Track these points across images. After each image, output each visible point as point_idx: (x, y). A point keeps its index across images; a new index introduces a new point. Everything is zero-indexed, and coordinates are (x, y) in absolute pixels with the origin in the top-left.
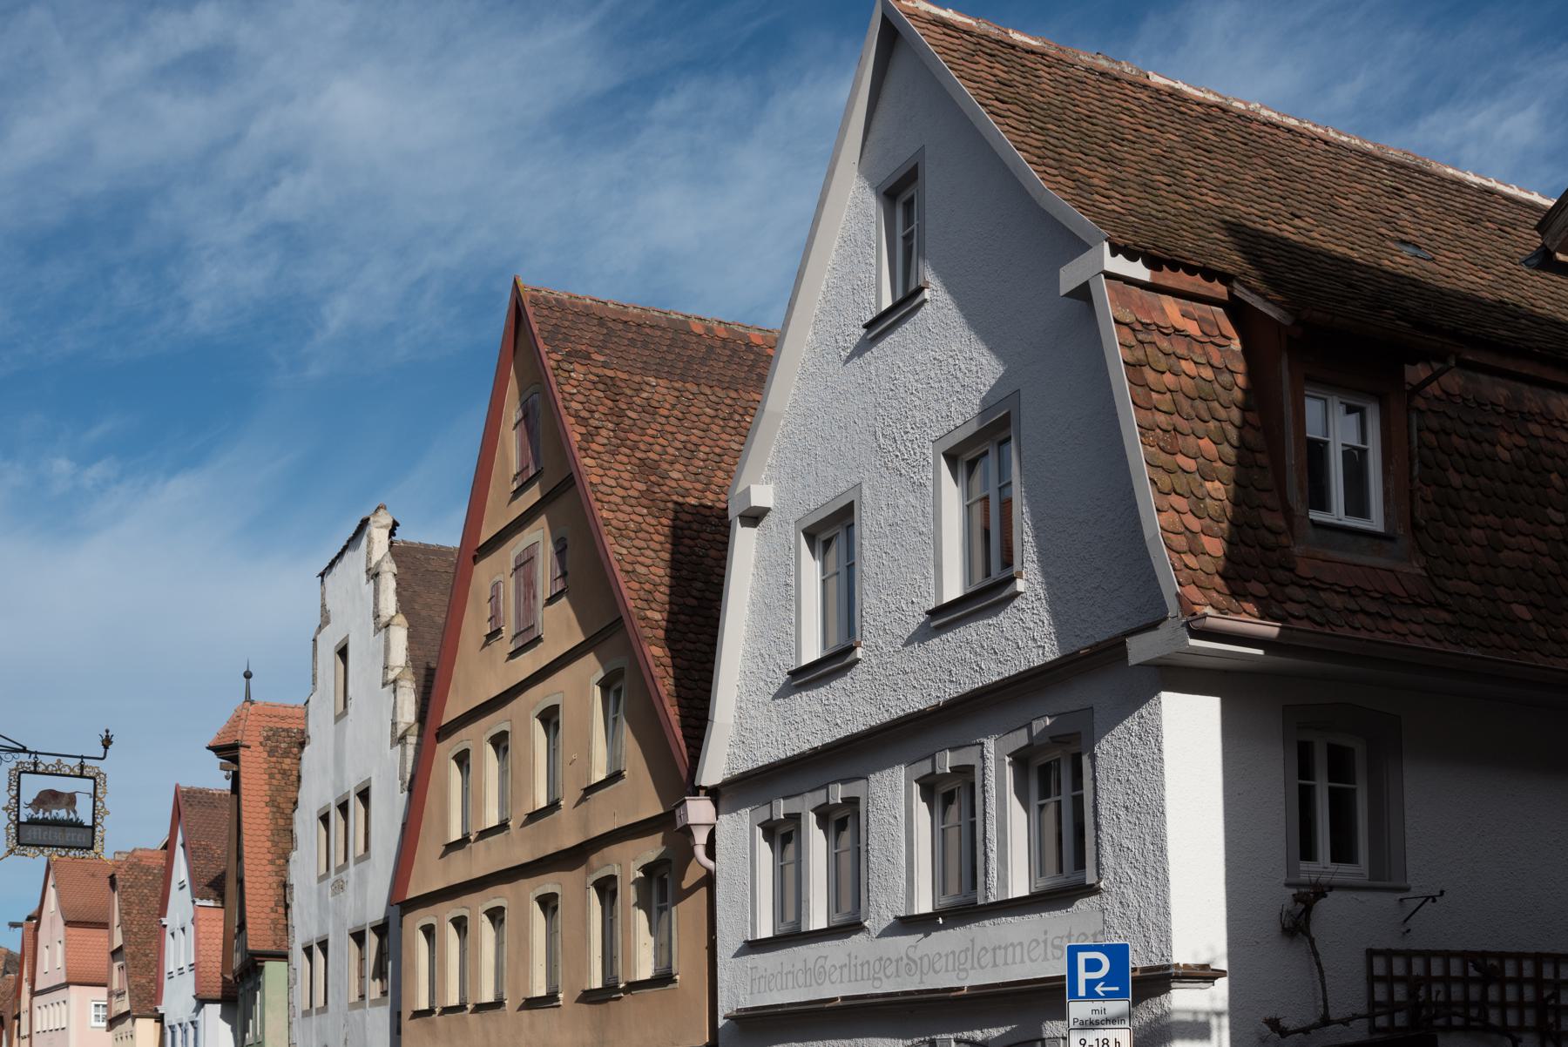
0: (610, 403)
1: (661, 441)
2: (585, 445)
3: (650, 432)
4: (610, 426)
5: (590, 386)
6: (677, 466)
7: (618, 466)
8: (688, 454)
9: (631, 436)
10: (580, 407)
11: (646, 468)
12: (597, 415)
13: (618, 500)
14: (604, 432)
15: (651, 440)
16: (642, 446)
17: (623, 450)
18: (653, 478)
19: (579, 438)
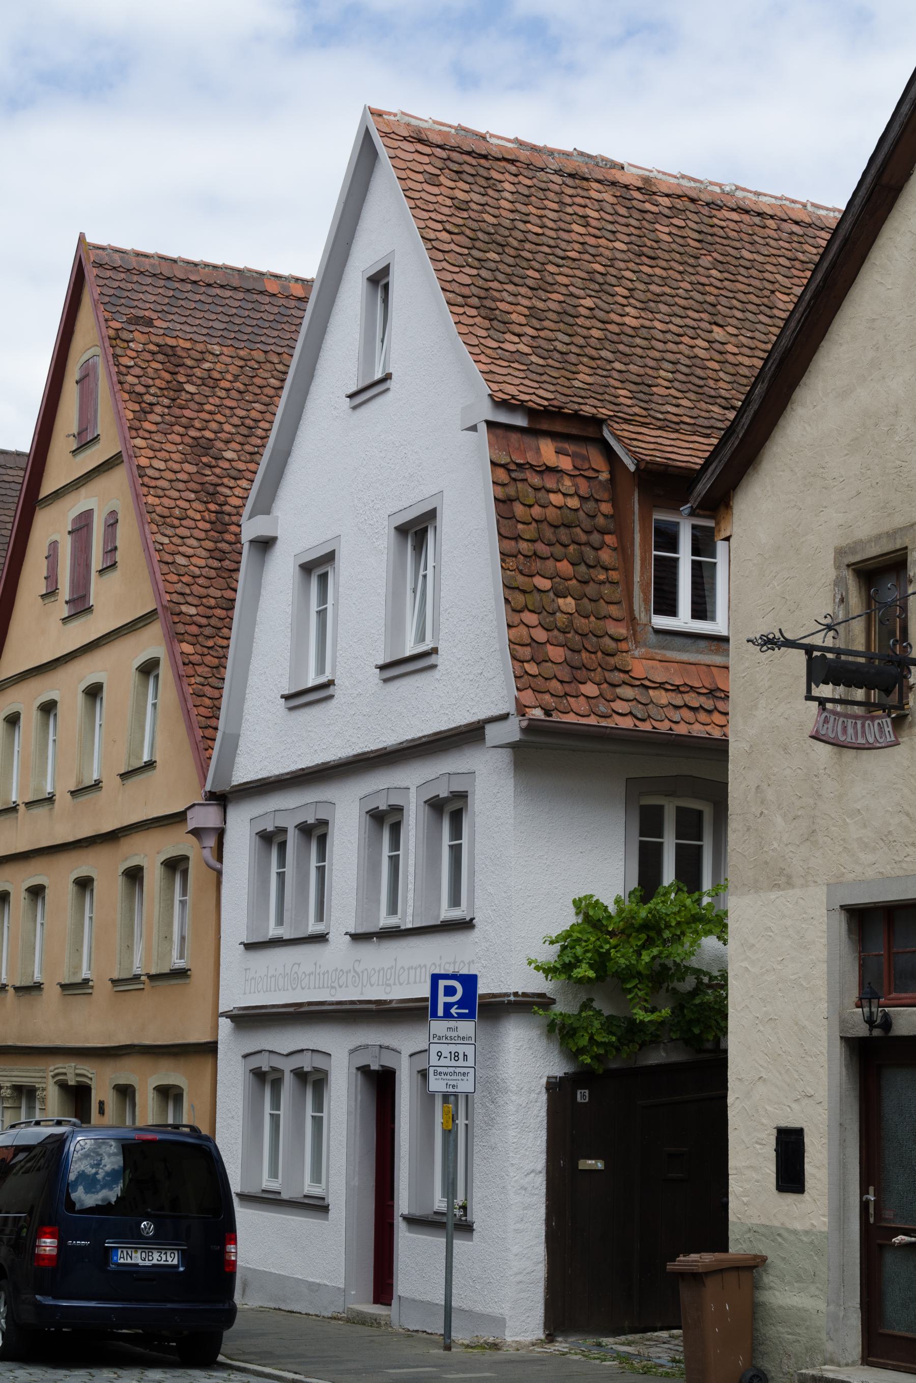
0: (167, 376)
1: (219, 417)
2: (137, 424)
3: (208, 407)
4: (166, 402)
5: (148, 356)
6: (233, 445)
7: (169, 447)
8: (244, 431)
9: (187, 413)
10: (136, 381)
11: (201, 449)
12: (152, 390)
13: (165, 484)
14: (158, 409)
15: (207, 416)
16: (197, 424)
17: (177, 428)
18: (205, 460)
19: (130, 415)
